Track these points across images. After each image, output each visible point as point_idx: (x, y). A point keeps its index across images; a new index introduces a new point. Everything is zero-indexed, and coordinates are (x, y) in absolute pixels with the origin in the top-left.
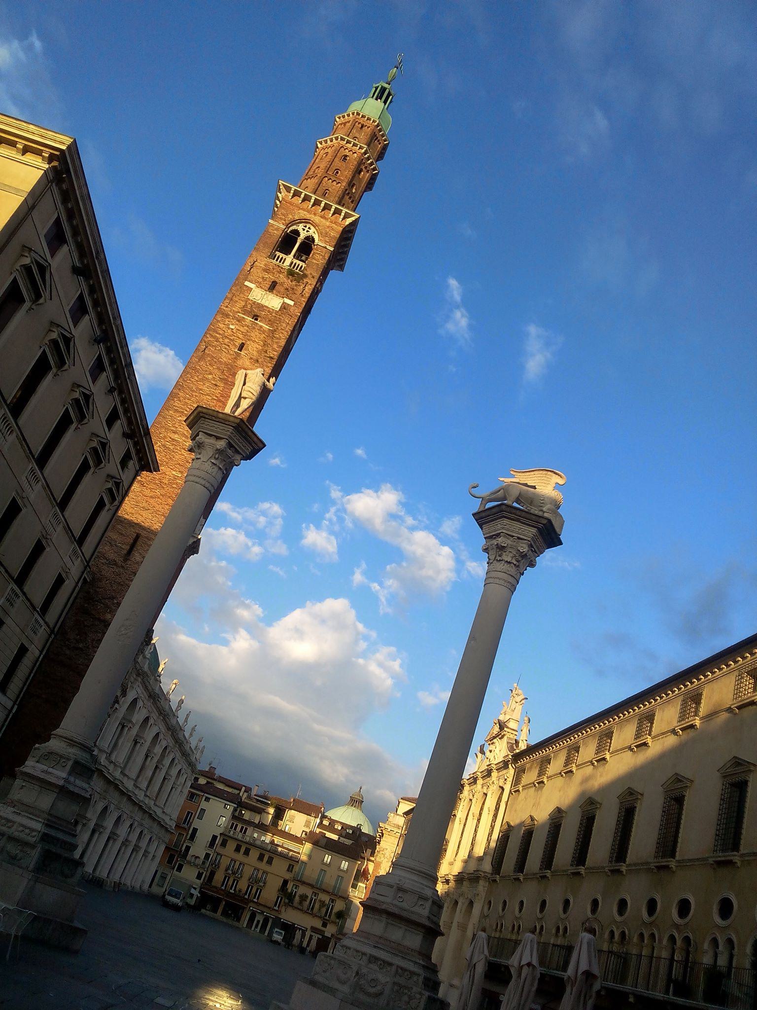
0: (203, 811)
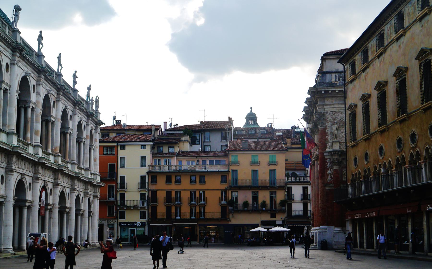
0: (123, 158)
